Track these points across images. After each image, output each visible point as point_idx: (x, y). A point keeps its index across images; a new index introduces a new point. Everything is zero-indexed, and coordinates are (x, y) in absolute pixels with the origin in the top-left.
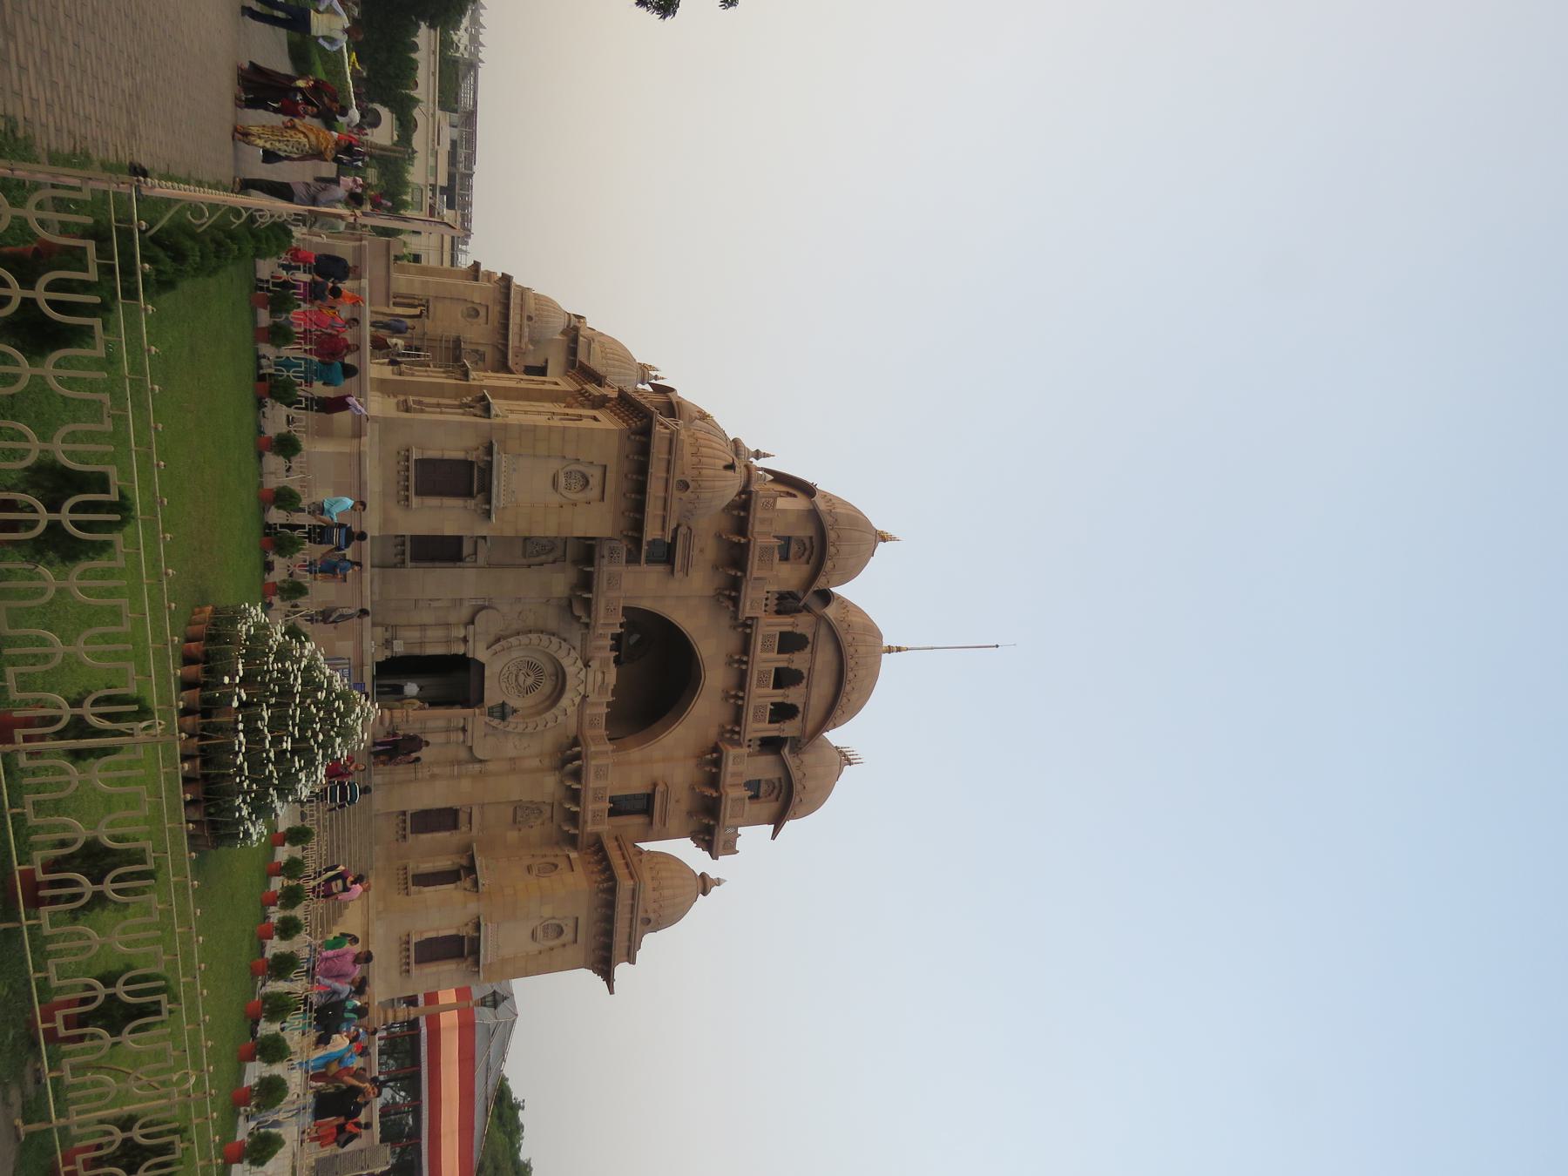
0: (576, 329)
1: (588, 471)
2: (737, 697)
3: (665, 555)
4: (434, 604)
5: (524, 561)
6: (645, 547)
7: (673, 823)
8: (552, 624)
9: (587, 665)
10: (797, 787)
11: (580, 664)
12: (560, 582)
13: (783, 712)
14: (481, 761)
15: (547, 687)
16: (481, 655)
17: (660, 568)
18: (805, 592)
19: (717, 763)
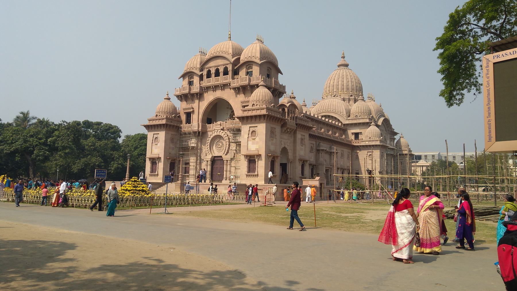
16: (209, 157)
19: (234, 89)
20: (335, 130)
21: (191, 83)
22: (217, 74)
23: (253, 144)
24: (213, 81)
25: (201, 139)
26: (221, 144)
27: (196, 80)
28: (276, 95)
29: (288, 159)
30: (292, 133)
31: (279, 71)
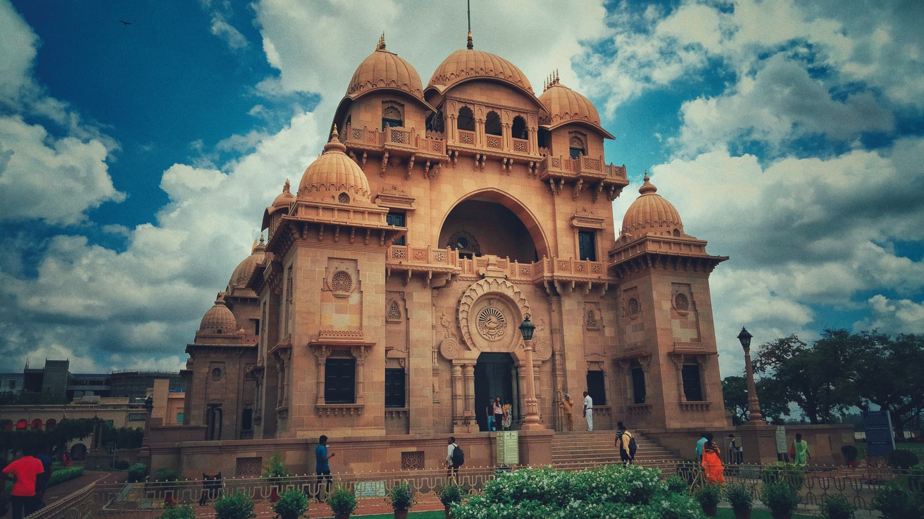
0: (226, 298)
1: (333, 270)
2: (508, 164)
3: (399, 216)
4: (437, 389)
5: (404, 323)
6: (394, 227)
7: (601, 213)
8: (451, 302)
9: (483, 277)
10: (576, 119)
11: (482, 282)
12: (420, 297)
13: (519, 129)
14: (553, 355)
15: (498, 307)
16: (474, 354)
17: (409, 220)
18: (427, 109)
19: (557, 180)
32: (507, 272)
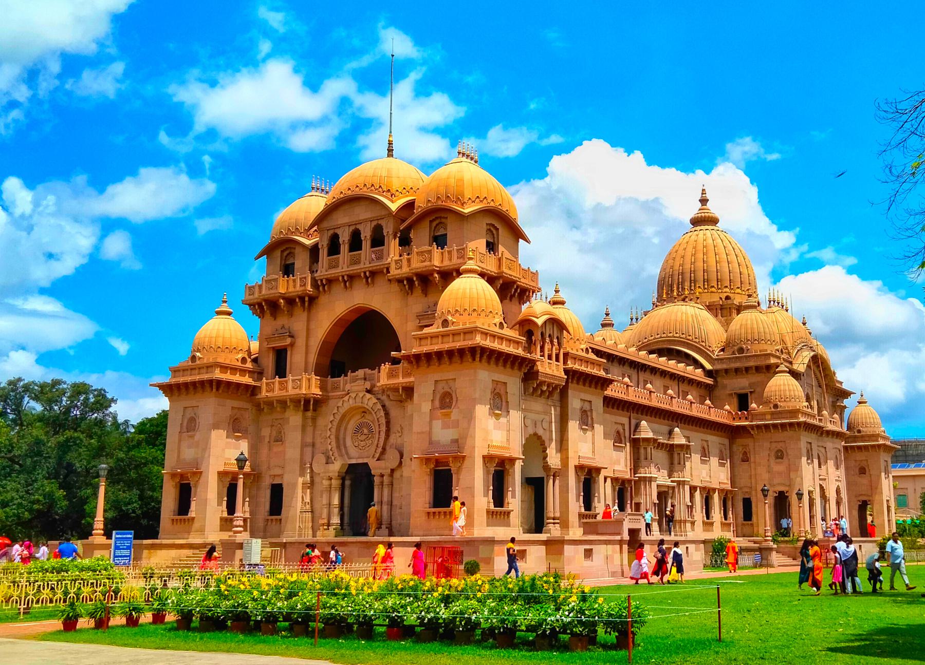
11: (346, 398)
16: (336, 467)
19: (400, 281)
20: (684, 387)
21: (288, 270)
22: (356, 243)
23: (445, 426)
24: (344, 263)
25: (314, 419)
26: (366, 431)
27: (301, 262)
28: (512, 297)
29: (546, 468)
30: (556, 396)
31: (517, 234)
32: (368, 385)
